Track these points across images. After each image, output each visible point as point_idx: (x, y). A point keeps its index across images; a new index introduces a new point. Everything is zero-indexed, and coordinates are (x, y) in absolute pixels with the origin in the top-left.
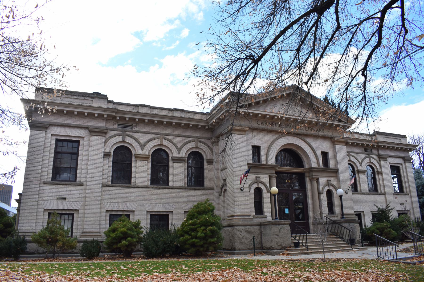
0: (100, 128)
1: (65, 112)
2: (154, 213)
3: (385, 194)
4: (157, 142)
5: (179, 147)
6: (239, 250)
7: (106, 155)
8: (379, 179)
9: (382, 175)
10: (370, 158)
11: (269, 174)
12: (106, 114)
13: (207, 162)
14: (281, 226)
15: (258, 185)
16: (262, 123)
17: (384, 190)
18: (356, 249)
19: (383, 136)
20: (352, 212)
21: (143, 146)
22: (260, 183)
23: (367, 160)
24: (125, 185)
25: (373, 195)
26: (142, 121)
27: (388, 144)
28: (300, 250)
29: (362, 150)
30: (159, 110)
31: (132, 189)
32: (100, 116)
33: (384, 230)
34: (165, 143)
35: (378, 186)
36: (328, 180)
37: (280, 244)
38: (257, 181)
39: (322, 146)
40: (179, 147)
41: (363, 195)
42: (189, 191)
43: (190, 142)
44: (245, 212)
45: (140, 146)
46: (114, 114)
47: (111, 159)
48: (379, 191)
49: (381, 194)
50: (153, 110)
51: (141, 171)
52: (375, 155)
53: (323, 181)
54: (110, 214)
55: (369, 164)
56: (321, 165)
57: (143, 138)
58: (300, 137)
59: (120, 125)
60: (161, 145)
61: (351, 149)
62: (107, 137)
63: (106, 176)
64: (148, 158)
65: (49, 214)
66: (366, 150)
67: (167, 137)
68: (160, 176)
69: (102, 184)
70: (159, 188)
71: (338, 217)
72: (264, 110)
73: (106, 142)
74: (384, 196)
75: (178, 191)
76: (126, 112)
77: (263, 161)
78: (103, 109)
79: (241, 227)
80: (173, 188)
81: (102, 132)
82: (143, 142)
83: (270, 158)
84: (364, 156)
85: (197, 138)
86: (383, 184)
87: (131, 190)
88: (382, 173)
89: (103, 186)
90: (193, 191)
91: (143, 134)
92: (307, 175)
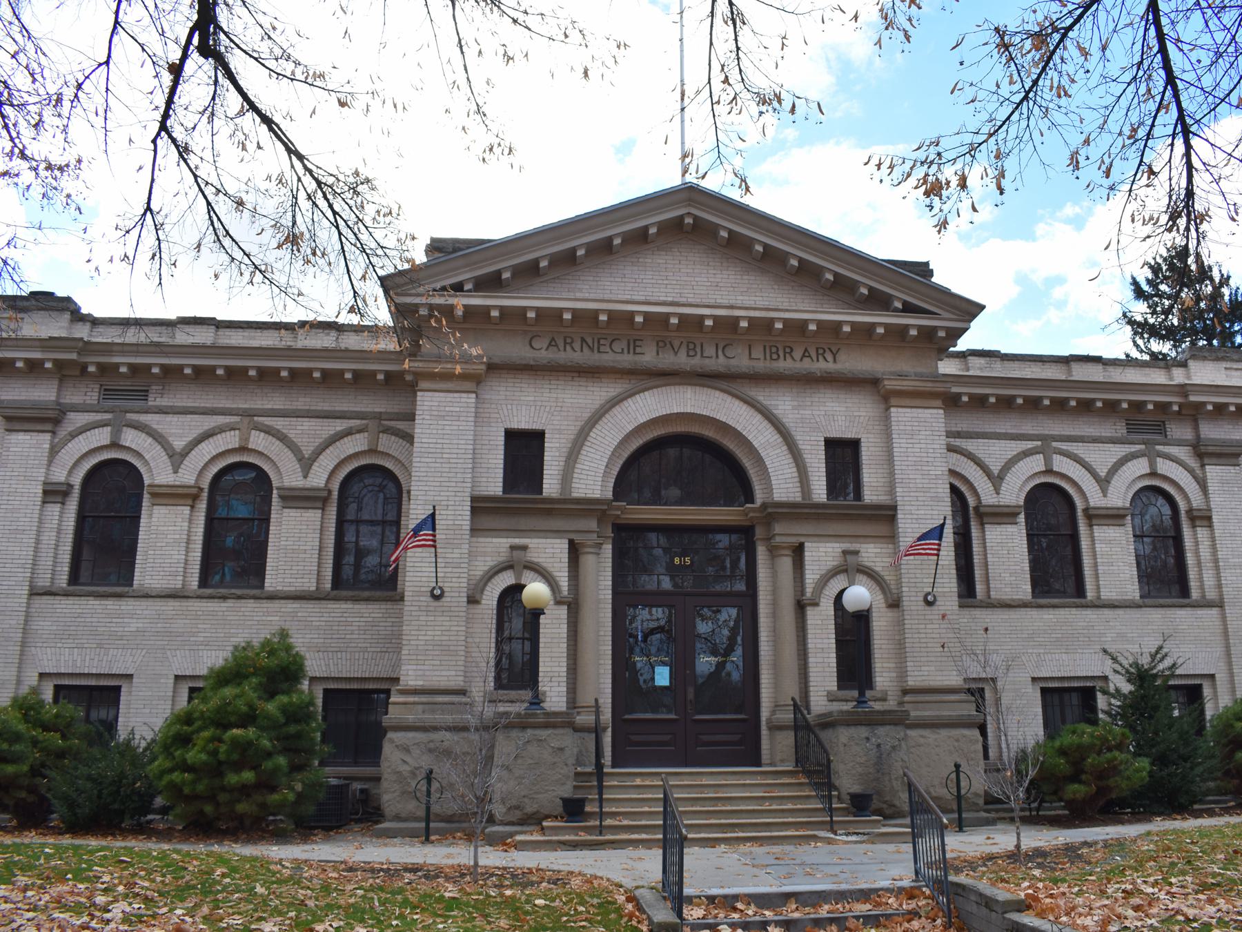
0: (35, 406)
1: (317, 375)
2: (67, 682)
3: (1219, 604)
4: (230, 440)
5: (305, 451)
6: (398, 818)
7: (54, 493)
8: (1197, 543)
9: (1210, 526)
10: (1152, 456)
11: (573, 536)
12: (49, 358)
13: (280, 497)
14: (530, 731)
15: (519, 576)
16: (552, 343)
17: (1219, 586)
18: (854, 838)
19: (1225, 364)
20: (954, 680)
21: (177, 458)
22: (526, 567)
23: (1139, 467)
24: (106, 589)
25: (1161, 611)
26: (171, 374)
27: (290, 358)
28: (588, 830)
29: (1117, 428)
30: (247, 333)
31: (131, 602)
32: (34, 367)
33: (1132, 758)
34: (258, 441)
35: (1192, 574)
36: (845, 553)
37: (514, 802)
38: (517, 562)
39: (843, 415)
40: (305, 451)
41: (1106, 611)
42: (332, 605)
43: (348, 433)
44: (448, 676)
45: (300, 460)
46: (74, 356)
47: (73, 505)
48: (1195, 594)
49: (1205, 604)
50: (228, 332)
51: (168, 541)
52: (1179, 443)
53: (821, 555)
54: (56, 686)
55: (1147, 482)
56: (820, 491)
57: (179, 430)
58: (724, 385)
59: (107, 393)
60: (243, 449)
61: (965, 423)
62: (63, 432)
63: (46, 562)
64: (195, 498)
65: (192, 690)
66: (1132, 427)
67: (268, 421)
68: (233, 558)
69: (32, 587)
70: (224, 598)
71: (885, 700)
72: (565, 295)
73: (54, 451)
74: (1214, 612)
75: (294, 605)
76: (115, 348)
77: (551, 486)
78: (37, 343)
79: (411, 735)
80: (273, 597)
81: (47, 420)
82: (179, 444)
83: (586, 471)
84: (1120, 451)
85: (379, 417)
86: (1216, 561)
87: (127, 605)
88: (1209, 518)
89: (34, 593)
90: (349, 605)
91: (182, 418)
92: (759, 532)
